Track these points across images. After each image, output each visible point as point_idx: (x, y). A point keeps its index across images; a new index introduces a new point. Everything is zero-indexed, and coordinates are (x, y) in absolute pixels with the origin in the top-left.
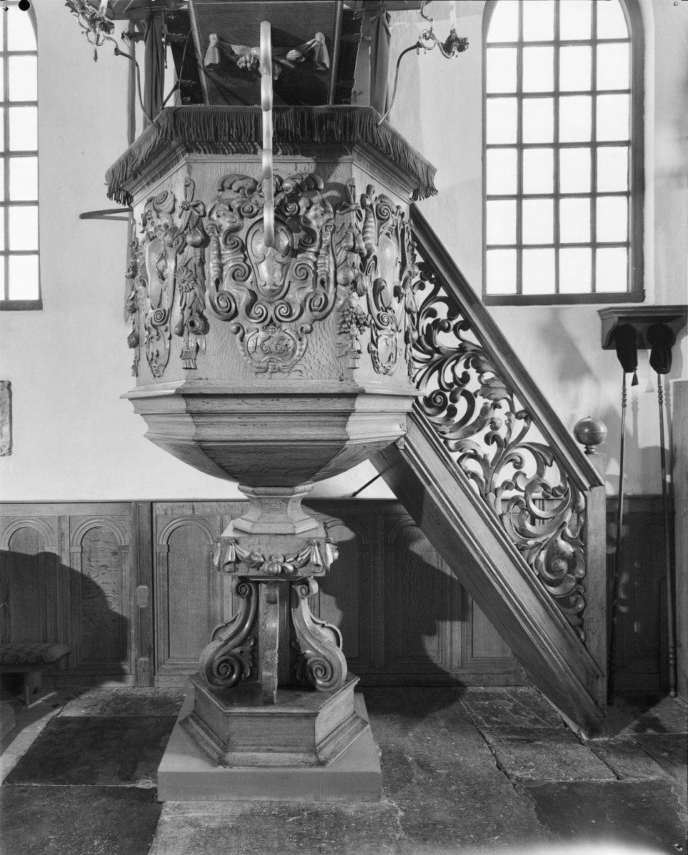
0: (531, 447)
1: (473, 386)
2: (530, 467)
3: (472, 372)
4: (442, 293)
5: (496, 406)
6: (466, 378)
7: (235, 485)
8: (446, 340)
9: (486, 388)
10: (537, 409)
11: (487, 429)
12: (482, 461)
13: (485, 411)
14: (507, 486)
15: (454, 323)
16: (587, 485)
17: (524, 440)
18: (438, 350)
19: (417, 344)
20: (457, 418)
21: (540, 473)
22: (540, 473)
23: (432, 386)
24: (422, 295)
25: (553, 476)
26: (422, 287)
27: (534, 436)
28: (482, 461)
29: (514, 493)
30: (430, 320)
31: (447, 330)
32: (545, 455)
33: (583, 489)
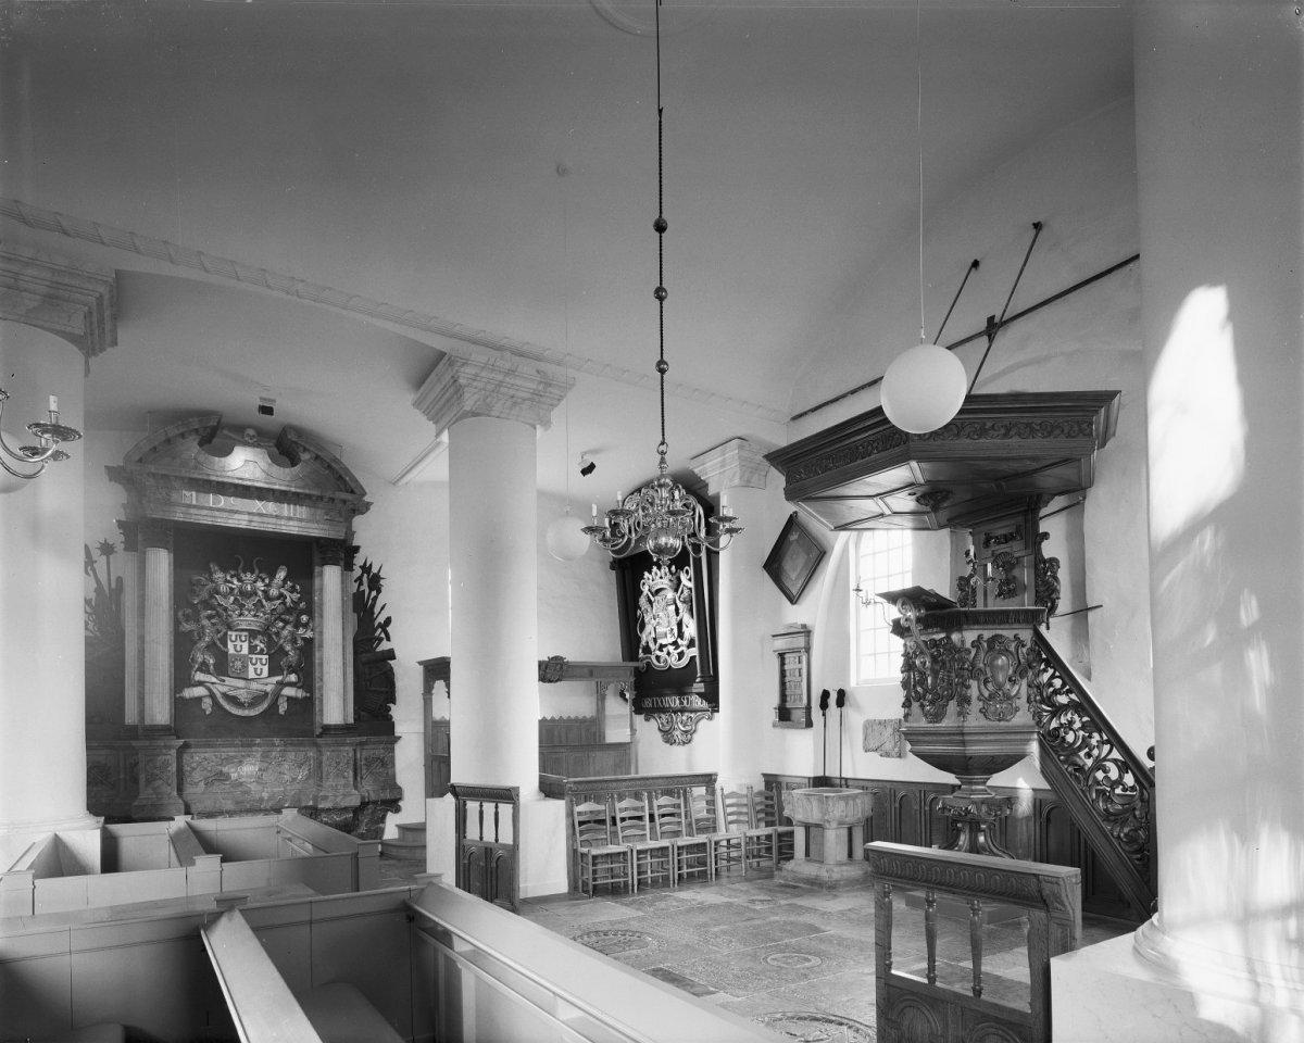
0: (1115, 761)
1: (1077, 725)
2: (1114, 774)
3: (1076, 717)
4: (1057, 674)
6: (1071, 722)
7: (953, 776)
8: (1063, 699)
9: (1083, 728)
10: (1116, 741)
11: (1087, 750)
16: (1147, 785)
17: (1109, 757)
18: (1052, 705)
19: (1043, 701)
21: (1121, 777)
22: (1121, 777)
23: (1054, 724)
24: (1045, 677)
25: (1129, 779)
26: (1045, 670)
27: (1116, 754)
30: (1051, 689)
31: (1060, 694)
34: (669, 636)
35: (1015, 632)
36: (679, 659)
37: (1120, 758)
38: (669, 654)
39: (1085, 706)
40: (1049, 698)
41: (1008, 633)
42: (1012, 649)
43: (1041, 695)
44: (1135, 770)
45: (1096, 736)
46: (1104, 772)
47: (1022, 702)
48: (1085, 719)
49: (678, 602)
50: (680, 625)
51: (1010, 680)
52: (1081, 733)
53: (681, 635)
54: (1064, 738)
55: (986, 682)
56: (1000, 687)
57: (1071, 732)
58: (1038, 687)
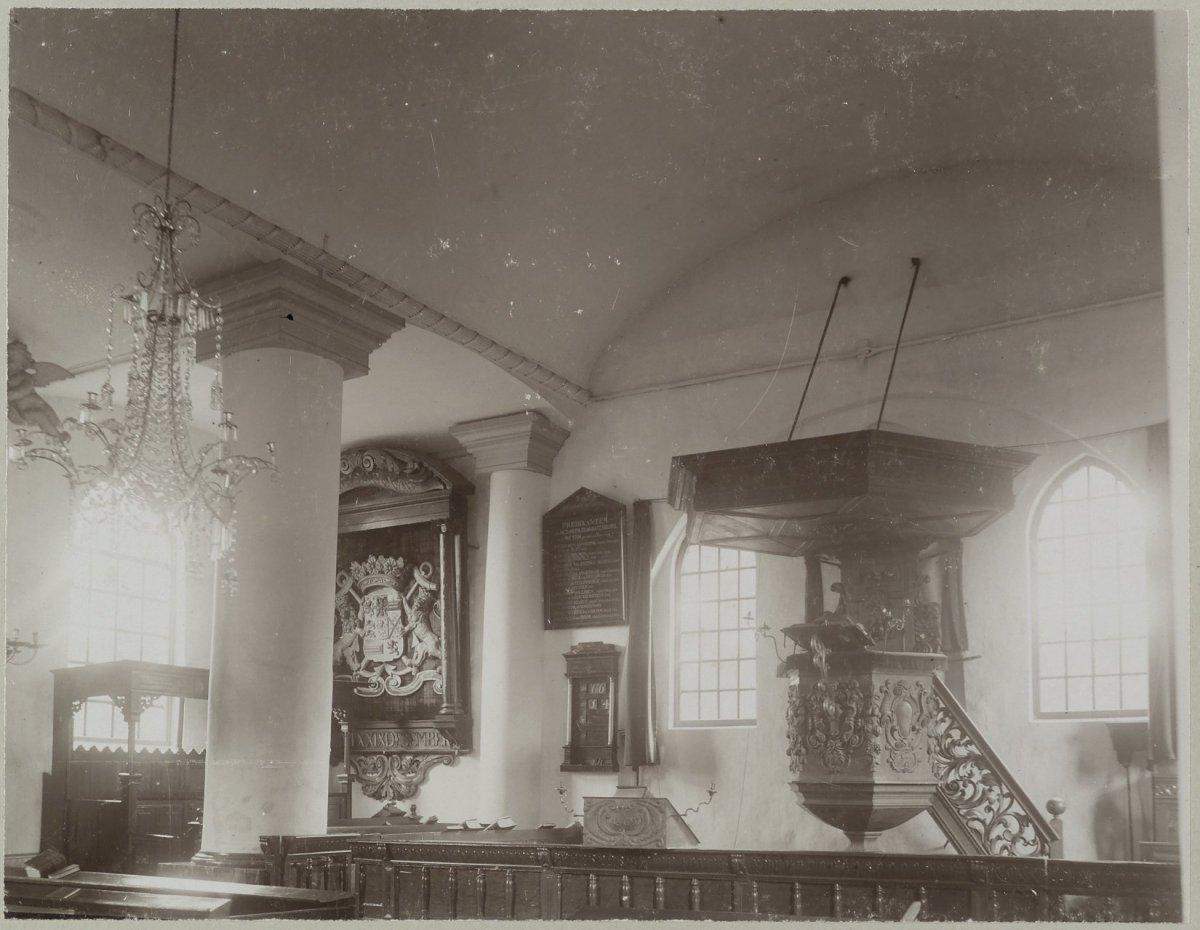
0: (1017, 816)
2: (1014, 827)
3: (975, 770)
5: (990, 790)
6: (971, 775)
8: (961, 752)
9: (984, 781)
10: (1016, 793)
11: (987, 803)
12: (983, 822)
13: (984, 792)
14: (999, 838)
15: (962, 742)
16: (1049, 840)
17: (1008, 812)
18: (952, 757)
19: (941, 753)
20: (967, 797)
21: (1021, 831)
22: (1021, 831)
23: (952, 777)
24: (942, 728)
25: (1030, 833)
26: (943, 721)
27: (1017, 808)
28: (983, 822)
29: (1004, 842)
30: (949, 740)
31: (959, 745)
32: (1023, 821)
33: (1047, 842)
34: (387, 651)
35: (918, 679)
36: (402, 685)
37: (1023, 813)
38: (384, 674)
39: (986, 759)
40: (948, 750)
41: (910, 680)
42: (915, 696)
43: (940, 745)
44: (1036, 823)
45: (996, 789)
46: (1006, 825)
47: (922, 754)
48: (986, 772)
49: (406, 607)
50: (407, 636)
51: (913, 729)
52: (981, 787)
53: (408, 651)
54: (963, 793)
55: (893, 730)
56: (903, 733)
57: (971, 786)
58: (937, 738)
